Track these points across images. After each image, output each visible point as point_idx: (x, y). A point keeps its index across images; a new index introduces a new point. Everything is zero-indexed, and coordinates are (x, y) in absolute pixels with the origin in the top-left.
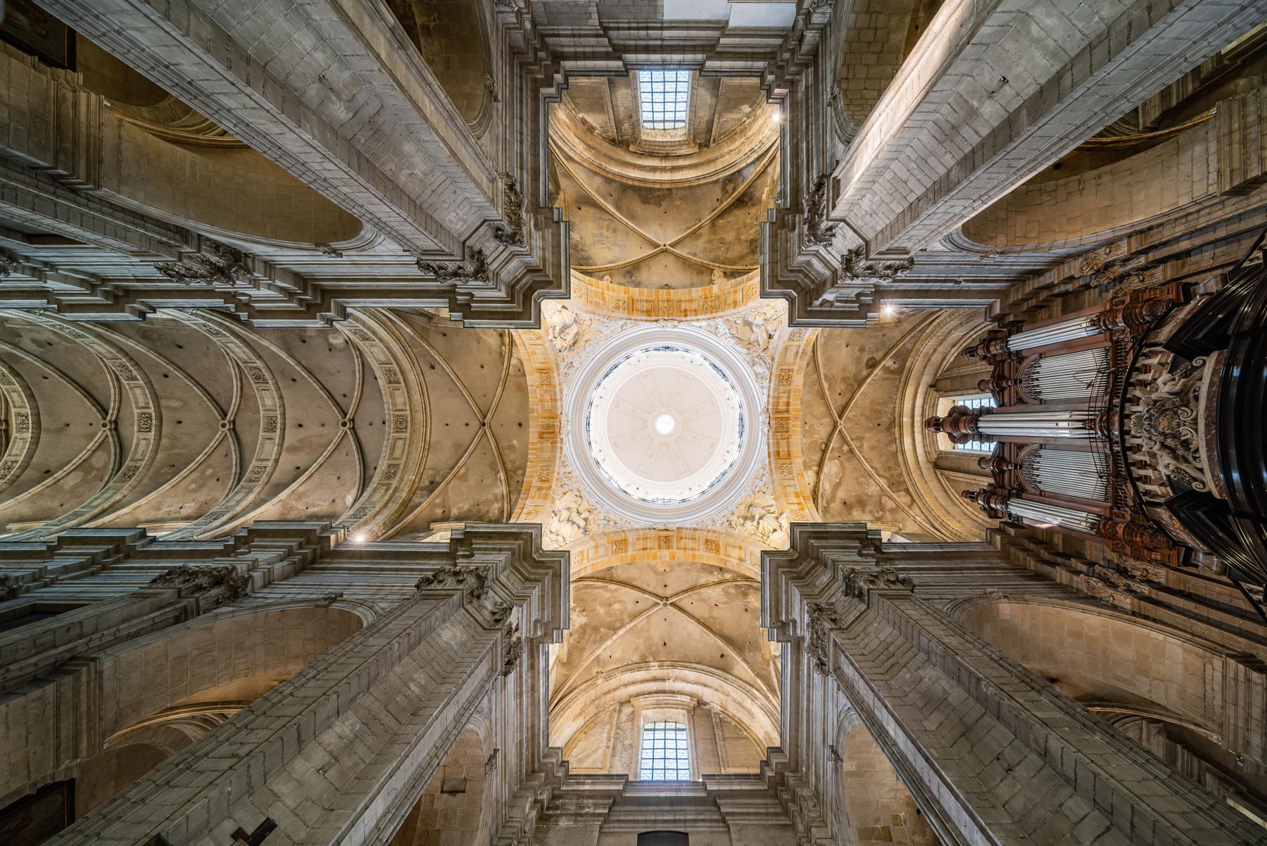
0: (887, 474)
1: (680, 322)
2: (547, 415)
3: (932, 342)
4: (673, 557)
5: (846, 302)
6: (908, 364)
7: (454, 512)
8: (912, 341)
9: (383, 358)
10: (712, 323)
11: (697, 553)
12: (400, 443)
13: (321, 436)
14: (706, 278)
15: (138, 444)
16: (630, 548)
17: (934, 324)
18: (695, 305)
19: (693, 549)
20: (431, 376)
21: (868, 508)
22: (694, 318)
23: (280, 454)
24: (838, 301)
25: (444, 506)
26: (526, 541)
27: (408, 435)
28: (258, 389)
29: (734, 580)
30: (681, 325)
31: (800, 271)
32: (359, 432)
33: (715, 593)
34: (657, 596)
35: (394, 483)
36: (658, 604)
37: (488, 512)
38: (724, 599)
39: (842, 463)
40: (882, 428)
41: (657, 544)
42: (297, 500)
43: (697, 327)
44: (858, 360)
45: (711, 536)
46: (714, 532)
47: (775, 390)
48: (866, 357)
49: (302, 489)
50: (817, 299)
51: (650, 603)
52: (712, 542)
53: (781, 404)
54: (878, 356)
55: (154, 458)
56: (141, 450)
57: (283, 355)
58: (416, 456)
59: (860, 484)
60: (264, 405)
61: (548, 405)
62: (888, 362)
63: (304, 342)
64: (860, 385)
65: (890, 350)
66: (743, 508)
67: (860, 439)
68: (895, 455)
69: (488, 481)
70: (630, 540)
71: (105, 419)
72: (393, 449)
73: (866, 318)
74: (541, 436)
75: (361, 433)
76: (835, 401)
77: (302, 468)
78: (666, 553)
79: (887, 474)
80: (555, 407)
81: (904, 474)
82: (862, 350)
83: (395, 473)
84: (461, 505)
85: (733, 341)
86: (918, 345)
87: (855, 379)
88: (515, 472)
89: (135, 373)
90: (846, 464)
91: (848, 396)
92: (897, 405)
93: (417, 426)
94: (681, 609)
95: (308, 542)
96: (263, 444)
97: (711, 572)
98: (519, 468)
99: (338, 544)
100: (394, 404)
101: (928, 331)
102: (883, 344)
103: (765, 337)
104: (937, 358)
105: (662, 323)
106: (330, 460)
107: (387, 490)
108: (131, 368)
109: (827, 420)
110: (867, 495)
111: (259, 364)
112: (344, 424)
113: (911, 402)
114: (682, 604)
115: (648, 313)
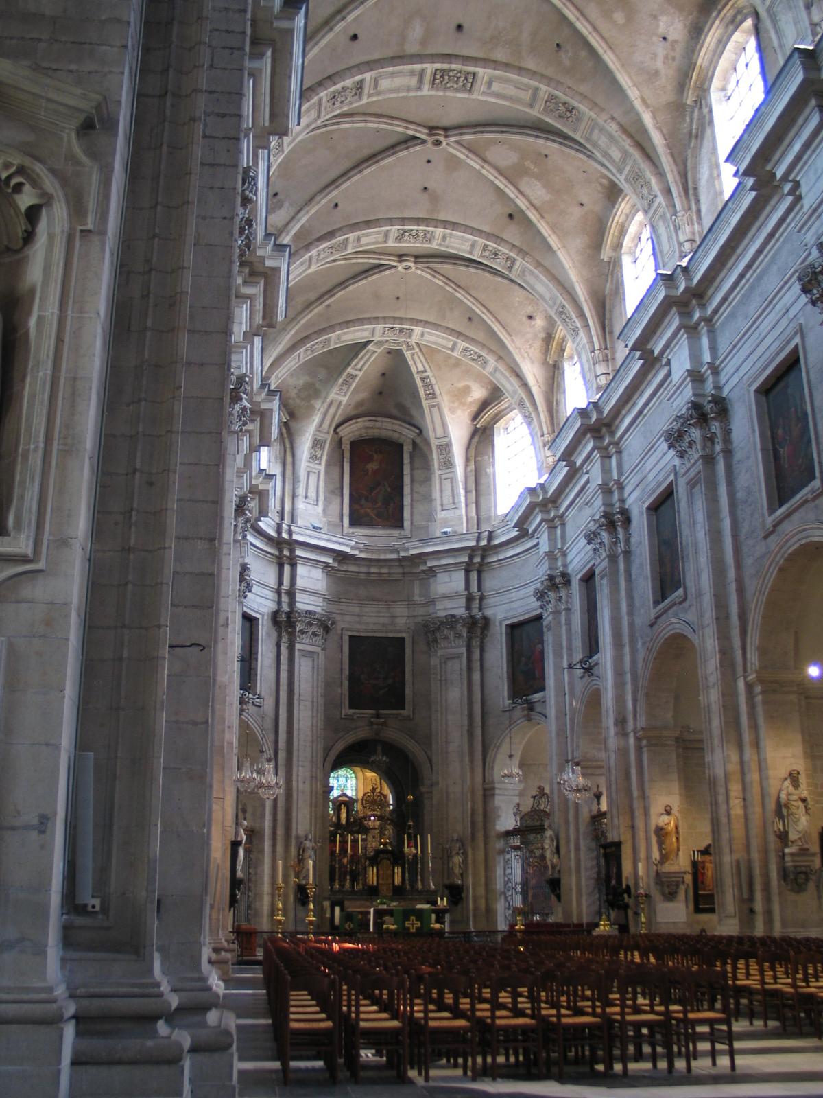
15: (498, 95)
55: (533, 74)
56: (511, 91)
71: (424, 142)
89: (348, 82)
108: (339, 86)
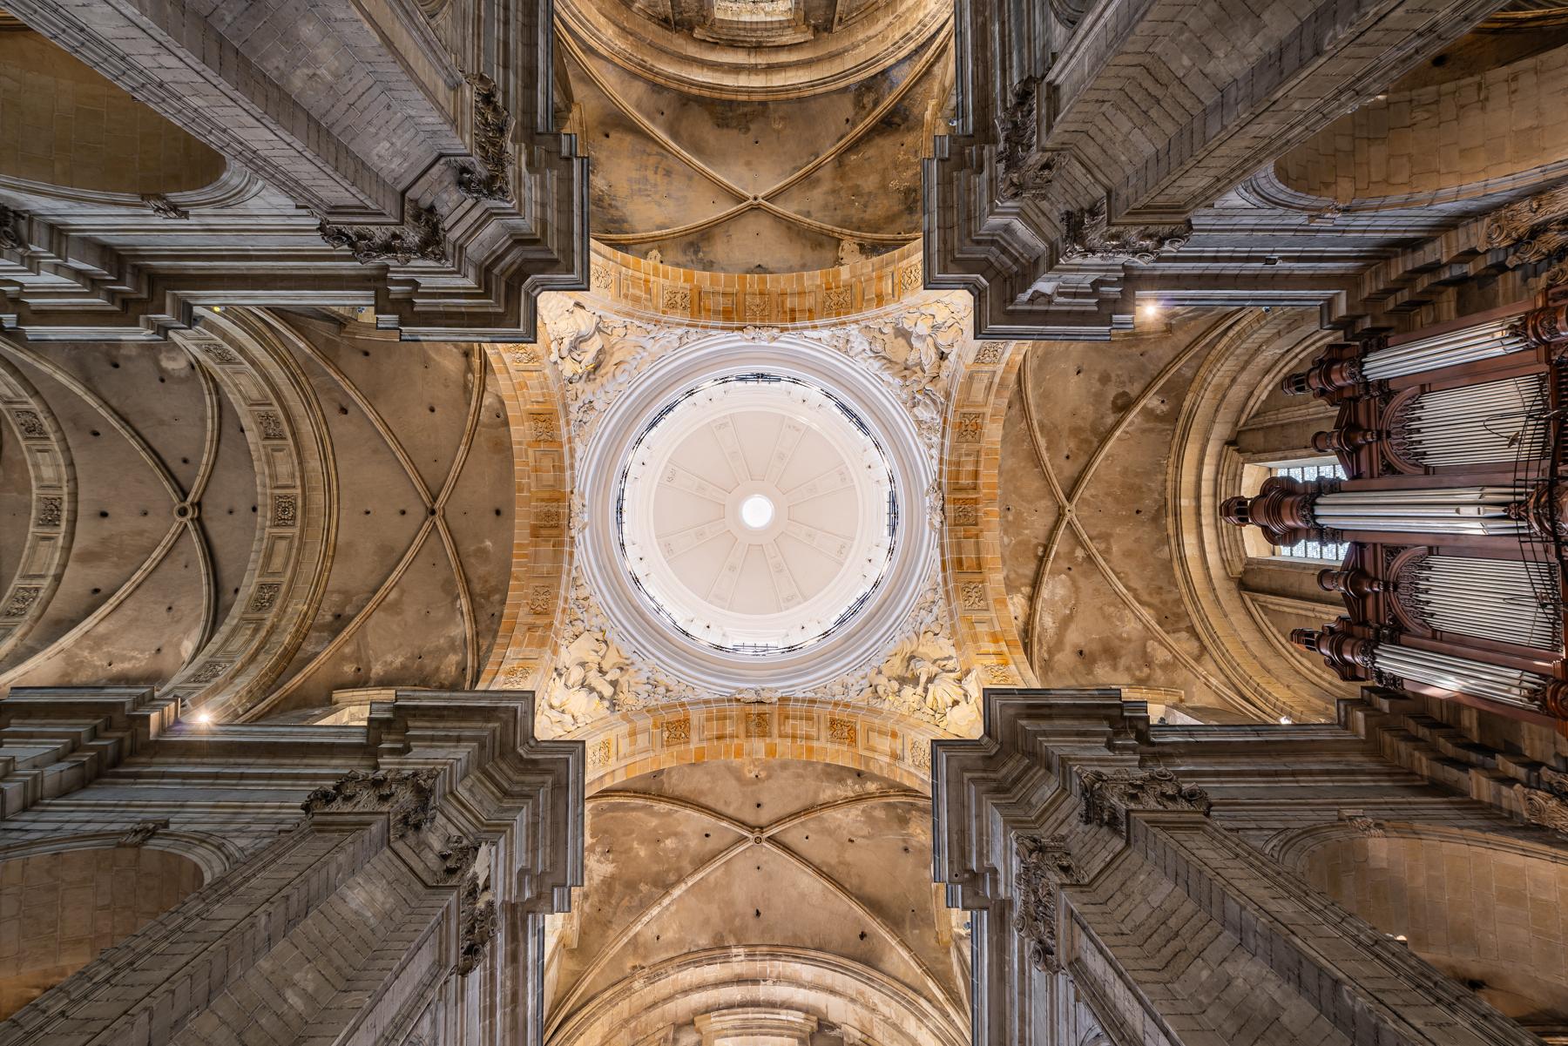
0: (1156, 600)
1: (783, 330)
2: (546, 495)
3: (1229, 366)
4: (771, 752)
5: (1075, 295)
6: (1187, 404)
7: (377, 670)
8: (1194, 364)
9: (255, 394)
10: (839, 332)
11: (815, 744)
12: (282, 546)
13: (141, 533)
14: (829, 255)
16: (694, 737)
17: (1231, 334)
18: (809, 302)
19: (808, 738)
20: (341, 426)
21: (1123, 662)
22: (808, 323)
23: (64, 566)
24: (1060, 294)
25: (358, 659)
26: (506, 723)
27: (296, 531)
28: (29, 450)
29: (884, 795)
30: (785, 337)
31: (993, 242)
32: (209, 525)
33: (847, 819)
34: (743, 824)
35: (270, 617)
36: (743, 839)
37: (438, 669)
38: (866, 830)
39: (1074, 582)
40: (1143, 517)
41: (742, 728)
42: (92, 650)
43: (815, 340)
44: (1098, 398)
45: (839, 714)
46: (847, 705)
47: (953, 449)
48: (1112, 391)
49: (102, 629)
50: (1024, 291)
51: (729, 839)
52: (843, 723)
53: (963, 475)
54: (1134, 390)
57: (78, 389)
58: (310, 569)
59: (1107, 618)
60: (39, 478)
61: (548, 477)
62: (1152, 401)
63: (116, 366)
64: (1103, 441)
65: (1155, 379)
66: (897, 661)
67: (1105, 537)
68: (1167, 566)
69: (438, 614)
70: (694, 722)
72: (269, 556)
73: (1110, 323)
74: (535, 532)
75: (214, 528)
76: (1059, 468)
77: (104, 591)
78: (759, 746)
79: (1156, 600)
80: (560, 481)
81: (1186, 599)
82: (1105, 379)
83: (271, 600)
84: (389, 658)
85: (877, 364)
86: (1202, 371)
87: (1094, 430)
88: (487, 598)
90: (1082, 583)
91: (1083, 460)
92: (1169, 477)
93: (314, 515)
94: (786, 848)
95: (109, 726)
96: (34, 548)
97: (841, 780)
98: (495, 590)
99: (163, 729)
100: (274, 477)
101: (1220, 346)
102: (1142, 369)
103: (934, 357)
104: (1237, 393)
105: (751, 332)
106: (156, 576)
107: (256, 631)
109: (1046, 503)
110: (1120, 638)
111: (33, 404)
112: (183, 512)
113: (1194, 472)
114: (789, 839)
115: (727, 314)
